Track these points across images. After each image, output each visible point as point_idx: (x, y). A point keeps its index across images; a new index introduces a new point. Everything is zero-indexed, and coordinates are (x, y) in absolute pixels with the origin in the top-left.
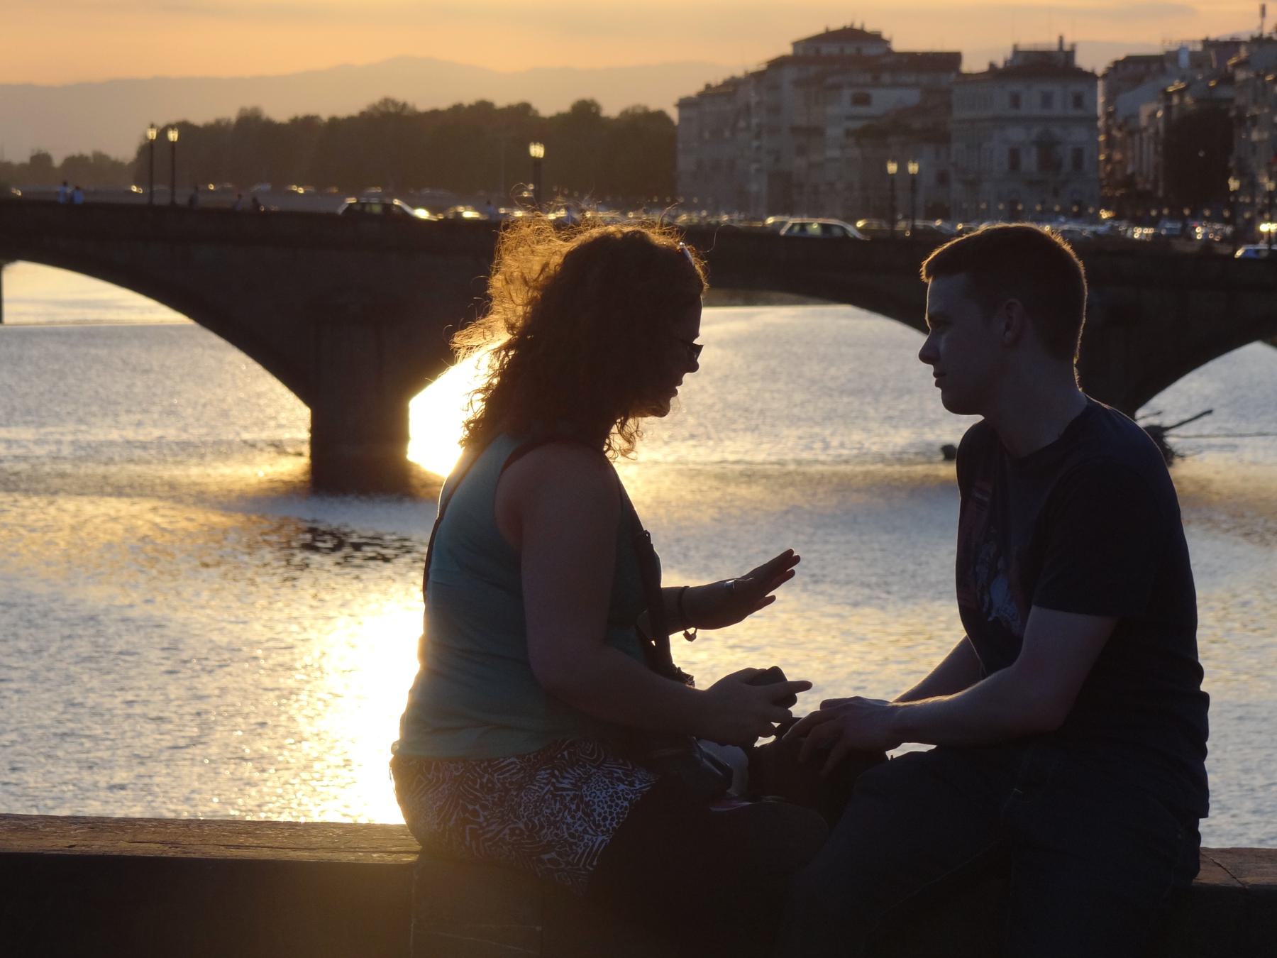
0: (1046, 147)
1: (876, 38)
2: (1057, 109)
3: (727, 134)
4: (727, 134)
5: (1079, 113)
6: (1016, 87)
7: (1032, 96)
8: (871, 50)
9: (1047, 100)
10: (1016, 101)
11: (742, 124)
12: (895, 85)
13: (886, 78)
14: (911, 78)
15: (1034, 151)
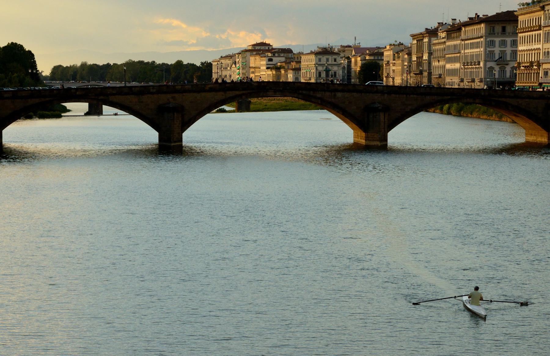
0: (327, 71)
1: (269, 45)
2: (330, 62)
3: (229, 68)
4: (229, 68)
5: (335, 63)
6: (319, 57)
7: (324, 59)
8: (267, 48)
9: (328, 60)
10: (320, 60)
11: (234, 66)
12: (279, 56)
13: (276, 55)
14: (282, 55)
15: (324, 72)
